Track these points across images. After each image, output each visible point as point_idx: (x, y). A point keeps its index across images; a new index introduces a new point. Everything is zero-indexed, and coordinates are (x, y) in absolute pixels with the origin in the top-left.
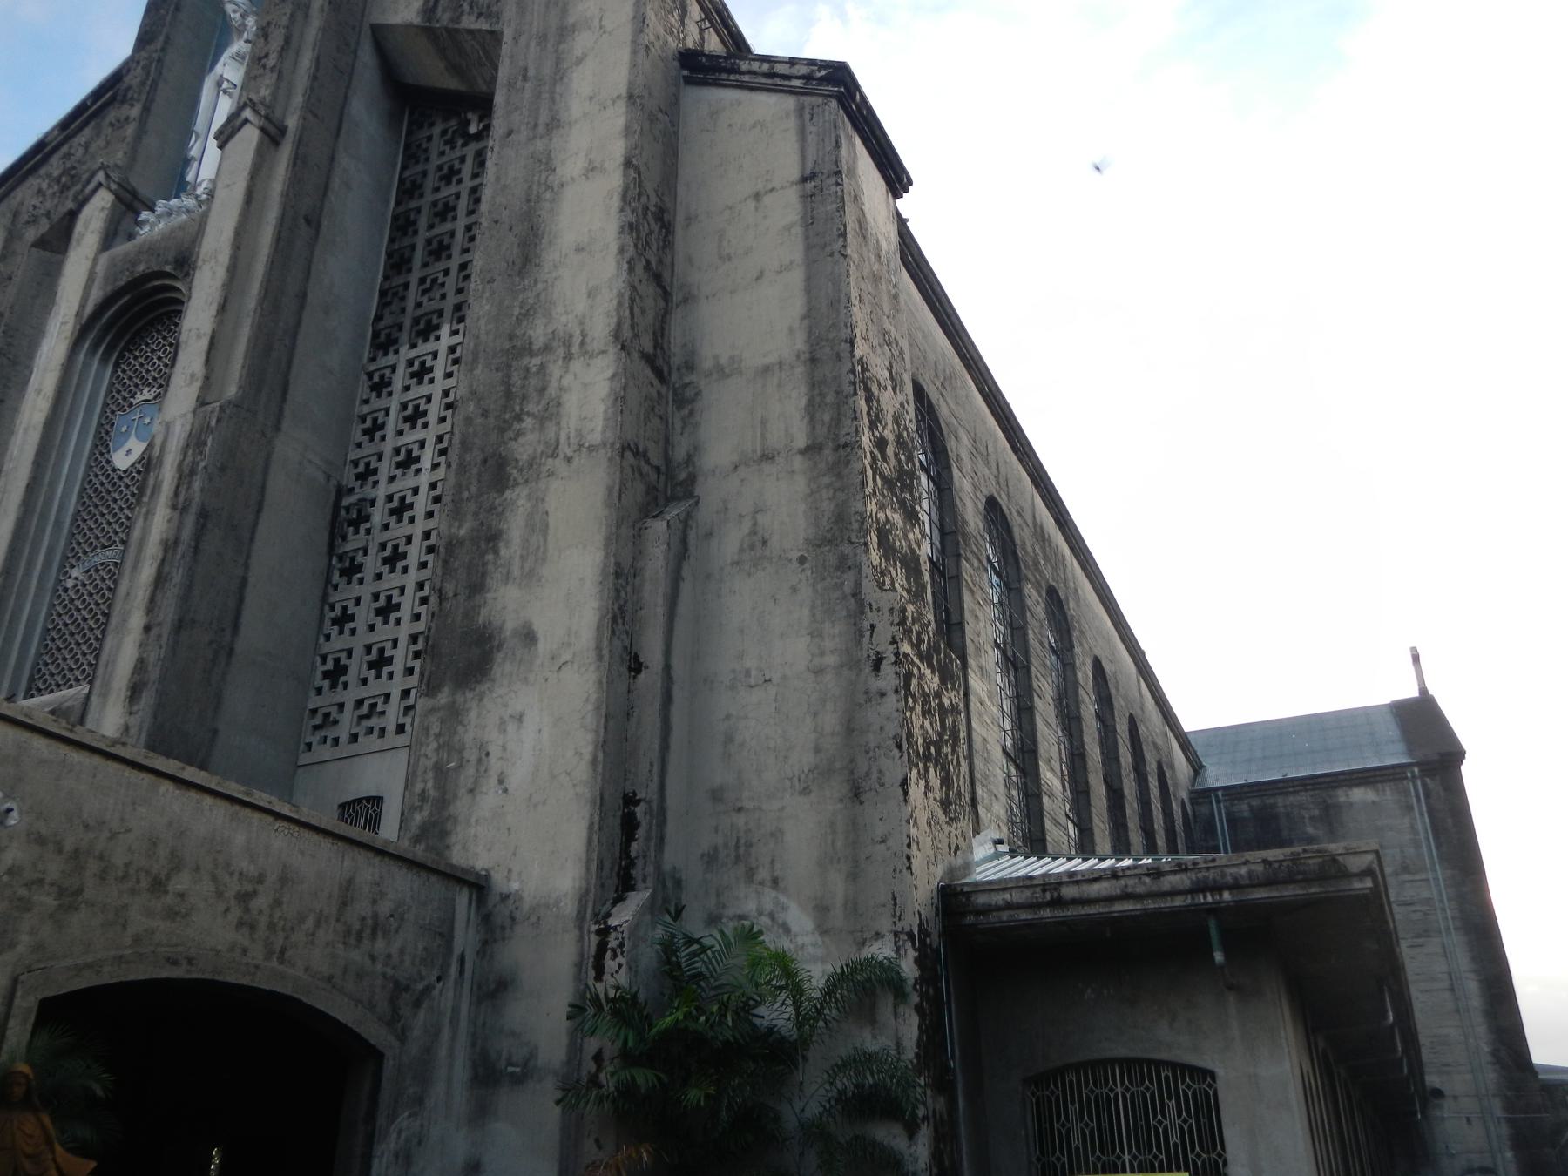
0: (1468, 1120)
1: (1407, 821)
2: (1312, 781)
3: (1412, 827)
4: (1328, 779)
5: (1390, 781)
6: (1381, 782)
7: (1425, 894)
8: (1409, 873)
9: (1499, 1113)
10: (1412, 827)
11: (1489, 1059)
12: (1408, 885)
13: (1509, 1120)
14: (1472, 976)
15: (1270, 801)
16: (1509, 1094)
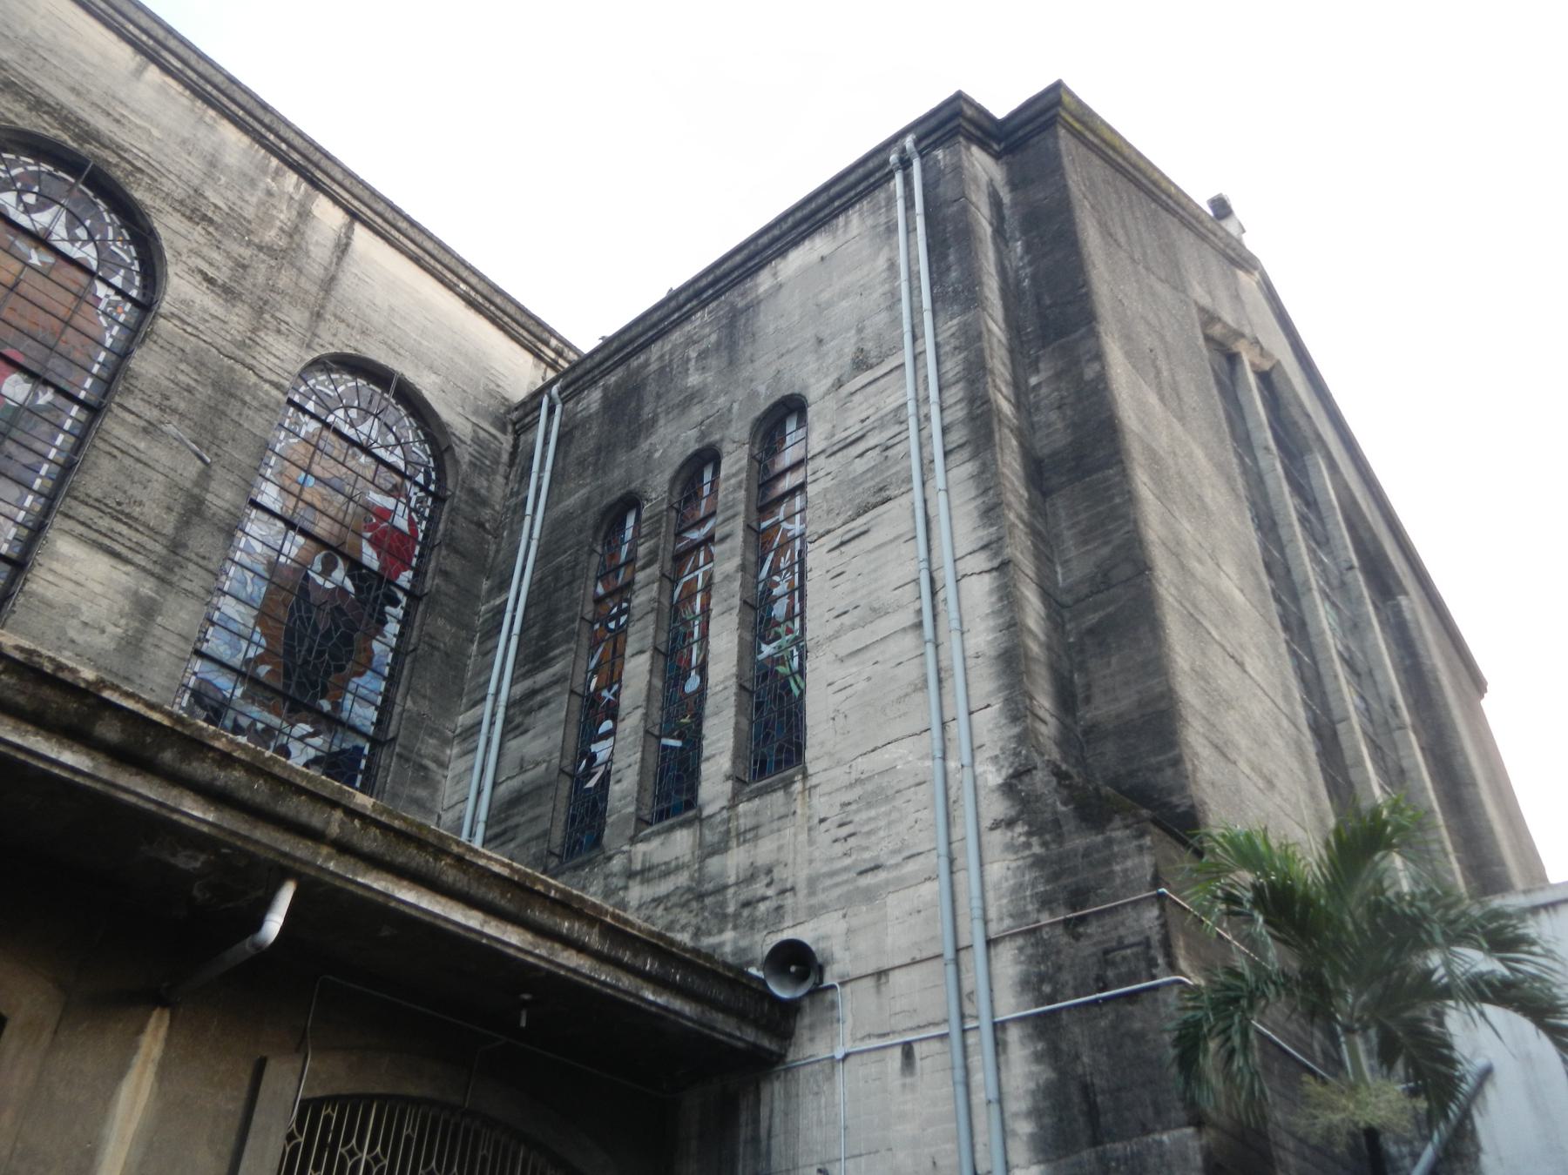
0: (908, 1050)
1: (881, 263)
2: (711, 278)
3: (892, 266)
4: (738, 258)
5: (860, 197)
6: (845, 208)
7: (892, 402)
8: (871, 367)
9: (1010, 1005)
10: (892, 266)
11: (997, 807)
12: (858, 398)
13: (1044, 1027)
14: (981, 561)
15: (635, 363)
16: (1046, 919)
